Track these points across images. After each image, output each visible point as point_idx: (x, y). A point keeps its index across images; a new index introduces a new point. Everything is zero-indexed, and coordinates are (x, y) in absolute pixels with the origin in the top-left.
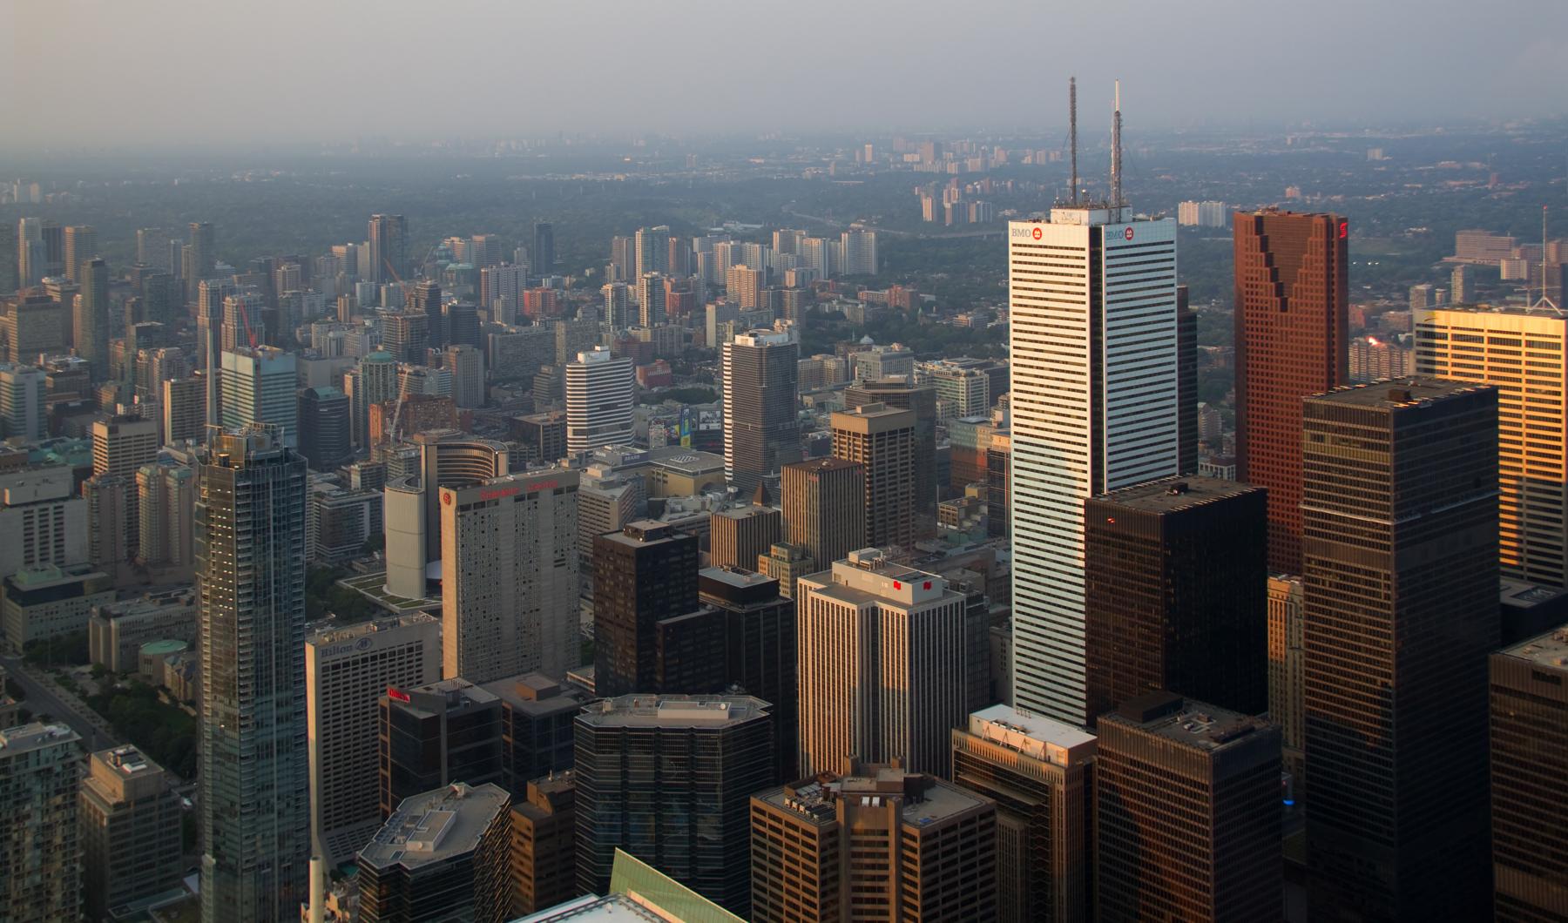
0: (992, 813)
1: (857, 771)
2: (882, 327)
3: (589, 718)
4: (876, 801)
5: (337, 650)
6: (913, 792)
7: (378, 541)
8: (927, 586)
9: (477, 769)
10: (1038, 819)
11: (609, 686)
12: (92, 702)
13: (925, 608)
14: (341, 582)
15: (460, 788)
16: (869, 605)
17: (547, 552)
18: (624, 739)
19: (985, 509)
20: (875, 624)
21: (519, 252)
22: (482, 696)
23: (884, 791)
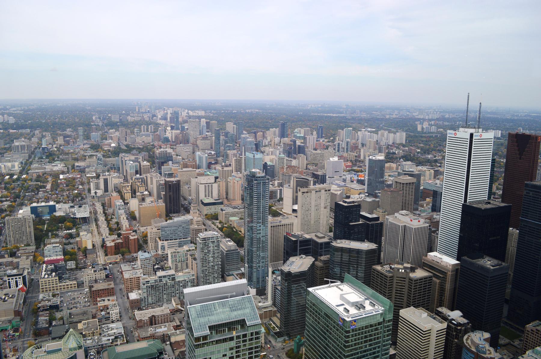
0: (432, 277)
1: (399, 264)
2: (406, 158)
3: (334, 244)
4: (403, 271)
5: (274, 223)
6: (413, 270)
7: (281, 199)
8: (419, 221)
9: (307, 253)
10: (443, 280)
11: (336, 238)
12: (219, 229)
13: (418, 227)
14: (273, 208)
15: (304, 256)
16: (404, 224)
17: (322, 205)
18: (342, 250)
19: (431, 204)
20: (405, 229)
21: (315, 133)
22: (307, 236)
23: (405, 268)
